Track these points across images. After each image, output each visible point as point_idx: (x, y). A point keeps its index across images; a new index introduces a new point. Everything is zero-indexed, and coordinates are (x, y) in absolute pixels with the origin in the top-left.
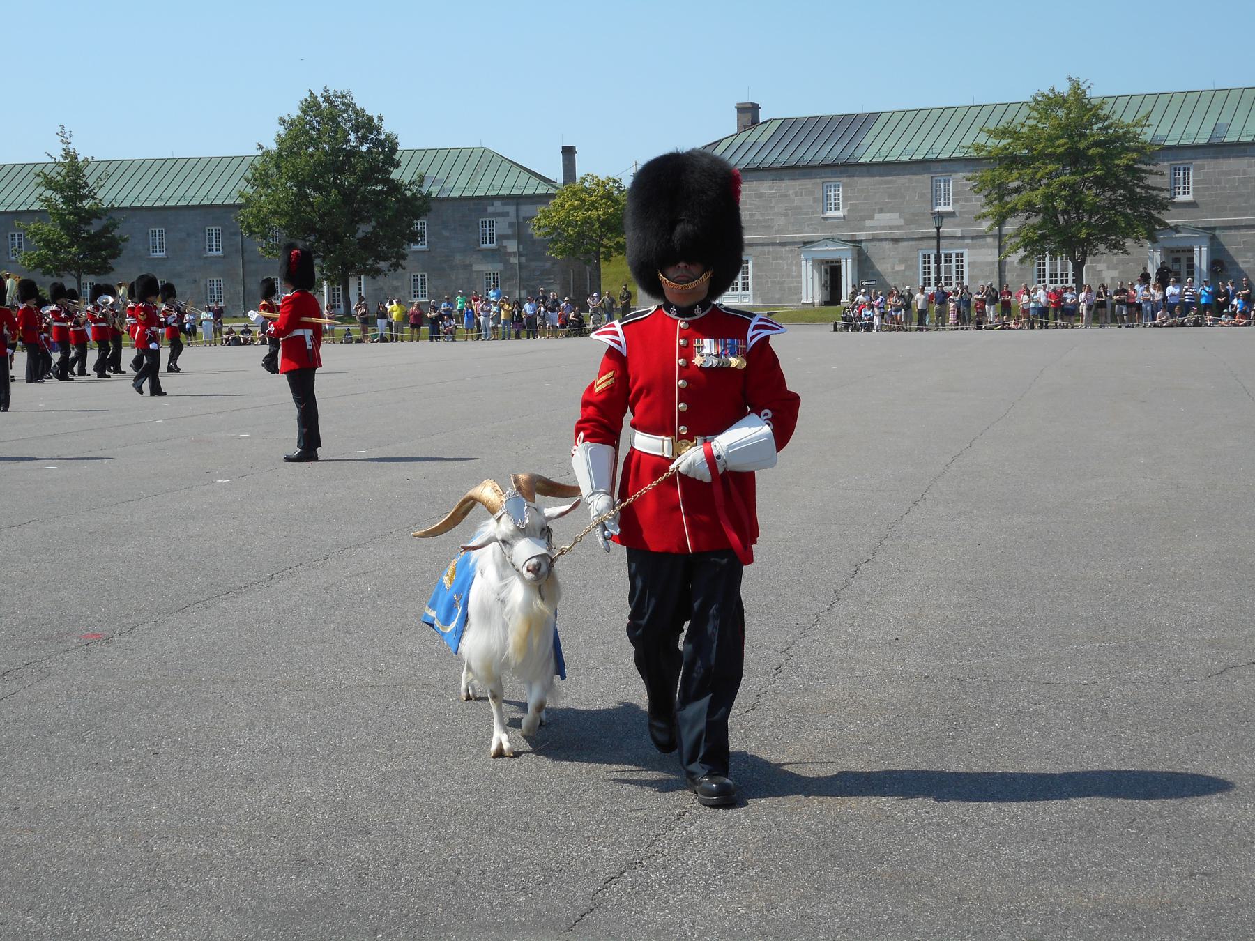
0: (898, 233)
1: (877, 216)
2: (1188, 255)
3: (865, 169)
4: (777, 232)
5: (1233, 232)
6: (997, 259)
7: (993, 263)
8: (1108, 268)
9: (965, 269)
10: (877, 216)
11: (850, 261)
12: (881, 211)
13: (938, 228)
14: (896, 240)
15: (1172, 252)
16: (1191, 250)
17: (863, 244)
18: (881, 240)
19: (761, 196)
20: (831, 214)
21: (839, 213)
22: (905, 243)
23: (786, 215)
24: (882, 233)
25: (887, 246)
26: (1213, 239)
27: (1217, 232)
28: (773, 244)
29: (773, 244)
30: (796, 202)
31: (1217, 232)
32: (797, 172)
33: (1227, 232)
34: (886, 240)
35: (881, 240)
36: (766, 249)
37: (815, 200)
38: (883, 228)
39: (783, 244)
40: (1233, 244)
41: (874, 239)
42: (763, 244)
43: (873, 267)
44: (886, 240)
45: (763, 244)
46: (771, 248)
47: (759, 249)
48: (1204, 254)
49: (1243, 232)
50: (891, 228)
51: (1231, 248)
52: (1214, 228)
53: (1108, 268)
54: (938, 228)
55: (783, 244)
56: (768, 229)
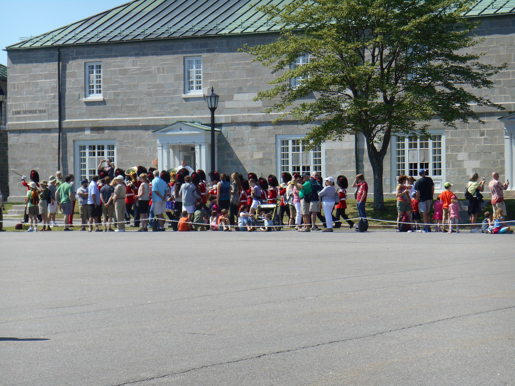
0: (258, 116)
1: (237, 96)
3: (224, 41)
4: (140, 114)
6: (354, 147)
7: (350, 150)
9: (323, 158)
10: (237, 96)
11: (203, 150)
12: (240, 90)
13: (213, 110)
14: (255, 124)
17: (224, 129)
18: (240, 124)
19: (124, 72)
20: (195, 93)
21: (200, 93)
22: (263, 128)
23: (149, 94)
24: (241, 116)
25: (246, 130)
28: (137, 128)
29: (137, 128)
30: (159, 81)
32: (160, 44)
34: (245, 124)
35: (240, 124)
36: (130, 132)
37: (177, 78)
38: (242, 110)
39: (146, 128)
41: (233, 123)
42: (127, 128)
43: (232, 154)
44: (245, 124)
45: (127, 128)
46: (135, 132)
47: (123, 132)
50: (249, 110)
54: (213, 110)
55: (146, 128)
56: (132, 110)
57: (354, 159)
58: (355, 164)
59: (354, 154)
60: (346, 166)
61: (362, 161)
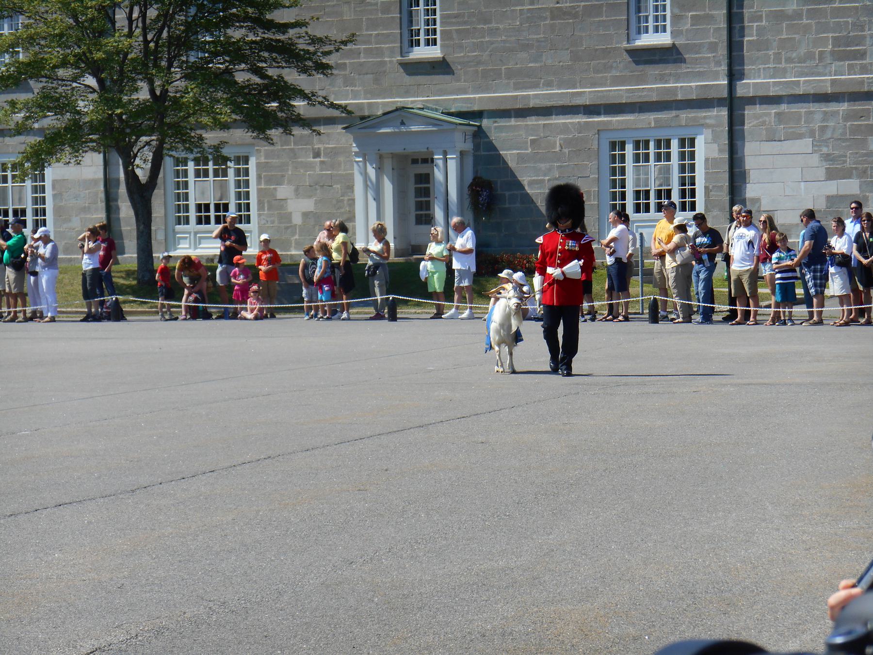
2: (422, 169)
5: (513, 122)
6: (101, 175)
7: (95, 182)
8: (297, 193)
9: (49, 194)
15: (415, 161)
16: (429, 161)
26: (479, 134)
27: (486, 123)
31: (486, 123)
33: (503, 122)
40: (512, 142)
48: (452, 165)
49: (532, 121)
51: (509, 155)
52: (478, 115)
53: (297, 193)
57: (102, 195)
58: (104, 204)
59: (102, 188)
60: (89, 208)
61: (116, 200)
